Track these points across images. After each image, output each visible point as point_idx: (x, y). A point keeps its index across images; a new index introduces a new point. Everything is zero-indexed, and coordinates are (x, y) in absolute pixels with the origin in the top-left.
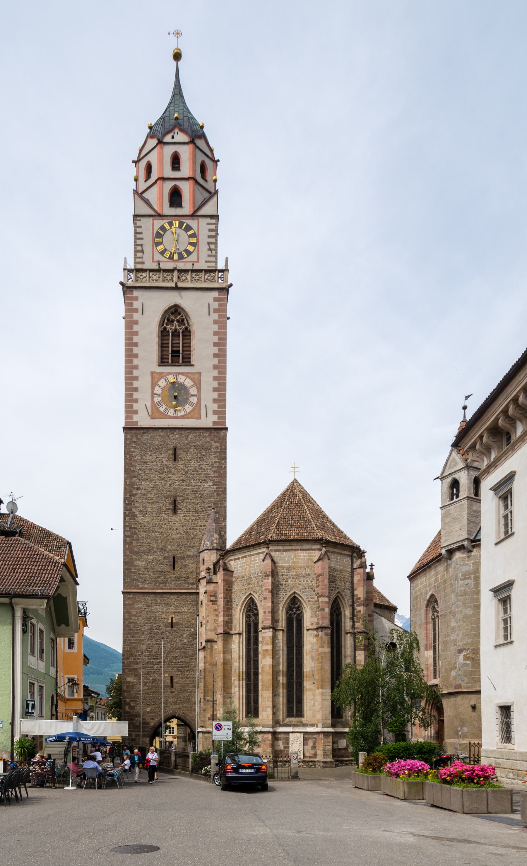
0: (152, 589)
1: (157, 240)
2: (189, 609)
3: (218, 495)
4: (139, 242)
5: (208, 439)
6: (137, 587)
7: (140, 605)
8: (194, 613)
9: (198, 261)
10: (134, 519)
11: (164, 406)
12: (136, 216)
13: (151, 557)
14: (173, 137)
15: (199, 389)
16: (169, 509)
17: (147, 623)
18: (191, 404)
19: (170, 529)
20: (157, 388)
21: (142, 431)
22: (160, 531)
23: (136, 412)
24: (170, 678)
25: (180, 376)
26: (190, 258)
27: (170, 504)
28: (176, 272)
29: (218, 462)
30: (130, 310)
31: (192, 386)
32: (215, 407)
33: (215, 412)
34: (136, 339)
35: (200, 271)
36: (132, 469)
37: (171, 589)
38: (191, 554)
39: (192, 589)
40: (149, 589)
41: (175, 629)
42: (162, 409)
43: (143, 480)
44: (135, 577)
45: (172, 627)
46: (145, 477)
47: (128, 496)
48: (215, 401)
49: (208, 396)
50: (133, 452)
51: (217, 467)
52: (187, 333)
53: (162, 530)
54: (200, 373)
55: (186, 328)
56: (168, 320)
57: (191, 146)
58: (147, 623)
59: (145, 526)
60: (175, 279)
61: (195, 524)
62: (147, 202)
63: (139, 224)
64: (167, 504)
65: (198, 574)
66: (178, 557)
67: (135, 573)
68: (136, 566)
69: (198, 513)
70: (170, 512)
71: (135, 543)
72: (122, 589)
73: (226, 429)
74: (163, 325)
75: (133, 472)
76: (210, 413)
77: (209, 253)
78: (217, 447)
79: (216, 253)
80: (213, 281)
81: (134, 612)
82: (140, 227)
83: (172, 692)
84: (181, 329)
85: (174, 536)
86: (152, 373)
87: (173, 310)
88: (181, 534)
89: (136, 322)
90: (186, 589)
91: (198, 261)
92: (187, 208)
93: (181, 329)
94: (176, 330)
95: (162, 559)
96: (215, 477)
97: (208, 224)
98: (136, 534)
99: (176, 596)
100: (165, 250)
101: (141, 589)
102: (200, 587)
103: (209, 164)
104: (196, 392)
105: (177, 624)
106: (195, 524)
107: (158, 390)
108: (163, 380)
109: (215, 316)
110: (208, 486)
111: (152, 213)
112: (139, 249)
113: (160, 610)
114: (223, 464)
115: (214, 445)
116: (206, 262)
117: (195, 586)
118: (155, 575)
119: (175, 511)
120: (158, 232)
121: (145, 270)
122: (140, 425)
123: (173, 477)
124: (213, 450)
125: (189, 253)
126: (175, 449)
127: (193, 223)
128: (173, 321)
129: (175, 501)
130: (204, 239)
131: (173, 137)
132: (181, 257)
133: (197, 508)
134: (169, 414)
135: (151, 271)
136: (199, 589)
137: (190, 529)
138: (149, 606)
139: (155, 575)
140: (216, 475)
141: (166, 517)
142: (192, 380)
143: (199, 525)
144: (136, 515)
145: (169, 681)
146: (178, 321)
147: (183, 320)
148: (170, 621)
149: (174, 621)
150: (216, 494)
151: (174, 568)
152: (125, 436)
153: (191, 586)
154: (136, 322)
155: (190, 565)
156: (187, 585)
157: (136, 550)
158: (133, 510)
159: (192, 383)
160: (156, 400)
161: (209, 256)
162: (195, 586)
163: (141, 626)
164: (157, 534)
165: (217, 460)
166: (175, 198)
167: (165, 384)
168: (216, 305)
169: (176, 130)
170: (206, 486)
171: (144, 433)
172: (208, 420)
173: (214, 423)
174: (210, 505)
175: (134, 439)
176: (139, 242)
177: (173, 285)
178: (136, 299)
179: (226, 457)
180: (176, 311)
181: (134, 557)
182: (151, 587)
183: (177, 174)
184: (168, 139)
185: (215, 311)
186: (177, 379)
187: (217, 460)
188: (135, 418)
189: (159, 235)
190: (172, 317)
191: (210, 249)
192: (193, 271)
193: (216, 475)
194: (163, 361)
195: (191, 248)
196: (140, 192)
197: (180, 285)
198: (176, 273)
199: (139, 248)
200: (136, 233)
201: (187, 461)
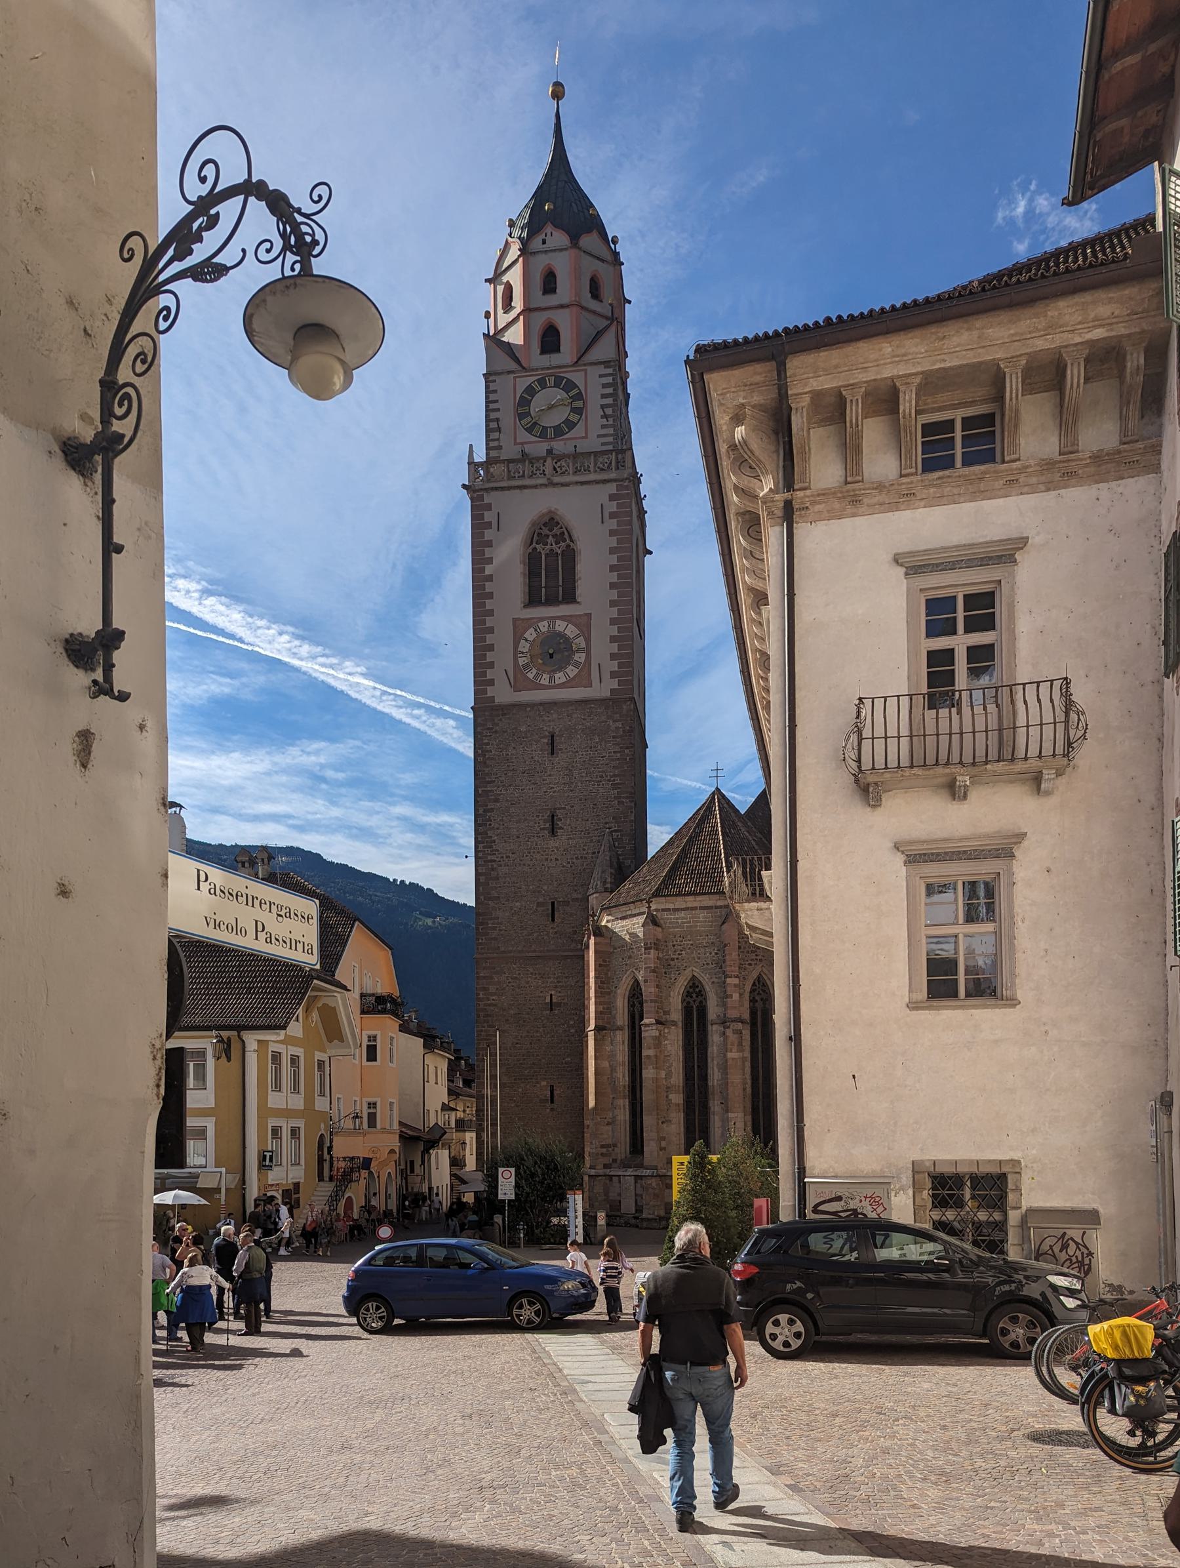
4: (493, 415)
9: (586, 437)
11: (534, 671)
14: (544, 242)
15: (588, 641)
22: (531, 863)
23: (491, 682)
25: (558, 622)
27: (545, 821)
31: (578, 636)
42: (531, 676)
50: (488, 744)
52: (570, 556)
60: (548, 470)
67: (494, 929)
71: (492, 884)
74: (531, 543)
77: (604, 422)
82: (495, 392)
83: (552, 1109)
86: (515, 620)
87: (546, 519)
91: (586, 437)
97: (600, 376)
105: (559, 1004)
107: (524, 646)
112: (493, 427)
116: (599, 436)
118: (525, 932)
119: (553, 832)
130: (595, 400)
131: (544, 242)
132: (559, 432)
139: (525, 932)
149: (554, 1000)
151: (553, 920)
157: (494, 894)
158: (490, 833)
160: (521, 661)
161: (603, 427)
164: (526, 869)
168: (613, 507)
175: (489, 725)
176: (493, 415)
183: (552, 300)
185: (613, 515)
186: (554, 626)
190: (545, 531)
191: (605, 416)
194: (533, 600)
195: (574, 418)
197: (556, 479)
199: (493, 425)
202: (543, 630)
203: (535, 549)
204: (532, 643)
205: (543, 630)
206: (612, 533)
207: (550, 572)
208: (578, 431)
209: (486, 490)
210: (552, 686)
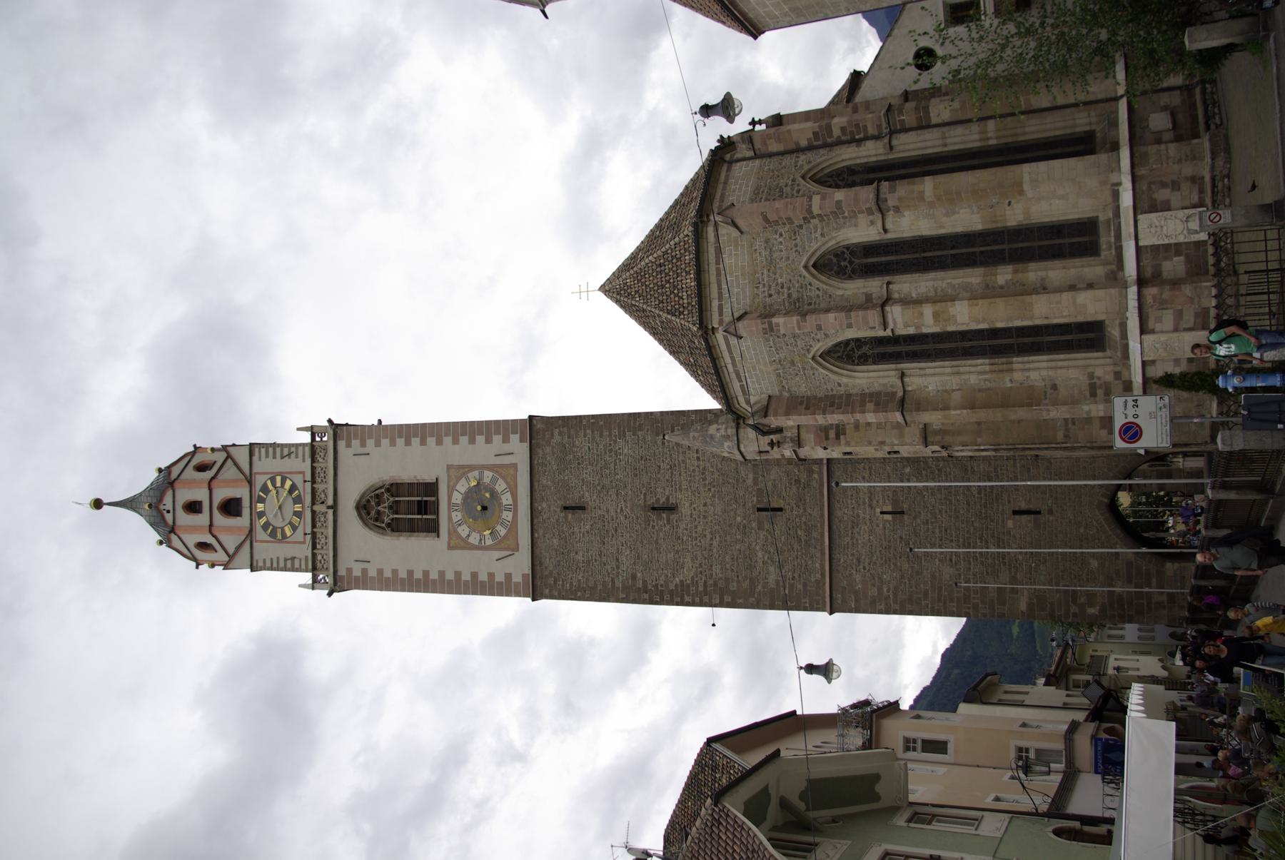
0: (823, 553)
1: (279, 536)
3: (640, 428)
4: (282, 565)
5: (548, 449)
6: (819, 583)
7: (858, 577)
9: (303, 473)
10: (688, 586)
12: (253, 569)
13: (760, 554)
15: (472, 468)
16: (668, 520)
17: (895, 565)
18: (494, 480)
19: (705, 517)
20: (471, 540)
21: (538, 568)
22: (709, 536)
24: (1017, 517)
25: (454, 501)
26: (300, 484)
27: (660, 518)
28: (315, 508)
30: (363, 582)
32: (497, 439)
33: (506, 440)
34: (403, 574)
35: (313, 469)
36: (600, 587)
37: (822, 516)
38: (751, 476)
39: (821, 474)
40: (823, 560)
41: (905, 506)
43: (618, 567)
44: (800, 587)
45: (903, 513)
46: (614, 564)
47: (646, 596)
48: (489, 440)
49: (483, 453)
52: (395, 488)
53: (707, 533)
54: (449, 467)
55: (388, 490)
56: (377, 520)
57: (177, 484)
58: (895, 565)
59: (701, 566)
62: (238, 548)
63: (260, 564)
64: (661, 523)
65: (790, 461)
66: (758, 502)
67: (791, 586)
68: (778, 585)
70: (674, 517)
72: (826, 614)
73: (531, 417)
75: (604, 584)
76: (506, 448)
77: (293, 456)
78: (560, 434)
79: (293, 445)
80: (325, 449)
81: (873, 592)
83: (1050, 512)
84: (388, 500)
85: (719, 510)
86: (450, 548)
87: (363, 512)
88: (713, 496)
89: (380, 572)
90: (822, 485)
91: (303, 473)
92: (242, 492)
93: (388, 500)
94: (390, 507)
95: (762, 534)
96: (610, 435)
98: (715, 584)
99: (837, 505)
100: (290, 523)
101: (823, 575)
102: (816, 457)
103: (198, 459)
104: (476, 473)
105: (895, 502)
107: (474, 539)
108: (460, 529)
109: (370, 443)
110: (627, 448)
111: (248, 542)
112: (289, 565)
113: (866, 536)
115: (557, 438)
117: (815, 468)
119: (671, 509)
120: (270, 535)
121: (314, 555)
122: (528, 571)
123: (612, 513)
124: (566, 439)
125: (293, 488)
126: (566, 508)
127: (259, 481)
128: (378, 512)
129: (653, 509)
133: (664, 466)
134: (510, 519)
135: (314, 547)
136: (821, 460)
137: (704, 479)
138: (859, 561)
139: (796, 547)
140: (606, 433)
141: (682, 526)
142: (458, 479)
143: (696, 463)
144: (682, 582)
145: (1024, 518)
146: (378, 504)
147: (377, 496)
148: (889, 517)
149: (889, 509)
151: (780, 510)
152: (547, 597)
153: (816, 476)
154: (380, 572)
156: (814, 483)
157: (746, 584)
158: (672, 587)
159: (463, 481)
160: (489, 542)
162: (815, 468)
163: (902, 577)
164: (715, 543)
166: (231, 507)
167: (464, 527)
169: (162, 507)
171: (541, 564)
172: (519, 451)
173: (522, 441)
174: (659, 443)
175: (551, 581)
176: (282, 565)
177: (331, 512)
178: (349, 570)
180: (365, 507)
181: (760, 587)
182: (818, 555)
184: (169, 517)
185: (363, 445)
186: (457, 505)
188: (517, 578)
189: (273, 534)
190: (373, 513)
191: (289, 455)
192: (313, 481)
193: (606, 433)
194: (432, 528)
195: (288, 484)
196: (227, 559)
197: (330, 502)
198: (315, 508)
200: (272, 569)
202: (460, 517)
203: (389, 525)
204: (472, 530)
205: (460, 517)
206: (378, 444)
207: (406, 509)
208: (298, 480)
209: (335, 572)
210: (514, 508)
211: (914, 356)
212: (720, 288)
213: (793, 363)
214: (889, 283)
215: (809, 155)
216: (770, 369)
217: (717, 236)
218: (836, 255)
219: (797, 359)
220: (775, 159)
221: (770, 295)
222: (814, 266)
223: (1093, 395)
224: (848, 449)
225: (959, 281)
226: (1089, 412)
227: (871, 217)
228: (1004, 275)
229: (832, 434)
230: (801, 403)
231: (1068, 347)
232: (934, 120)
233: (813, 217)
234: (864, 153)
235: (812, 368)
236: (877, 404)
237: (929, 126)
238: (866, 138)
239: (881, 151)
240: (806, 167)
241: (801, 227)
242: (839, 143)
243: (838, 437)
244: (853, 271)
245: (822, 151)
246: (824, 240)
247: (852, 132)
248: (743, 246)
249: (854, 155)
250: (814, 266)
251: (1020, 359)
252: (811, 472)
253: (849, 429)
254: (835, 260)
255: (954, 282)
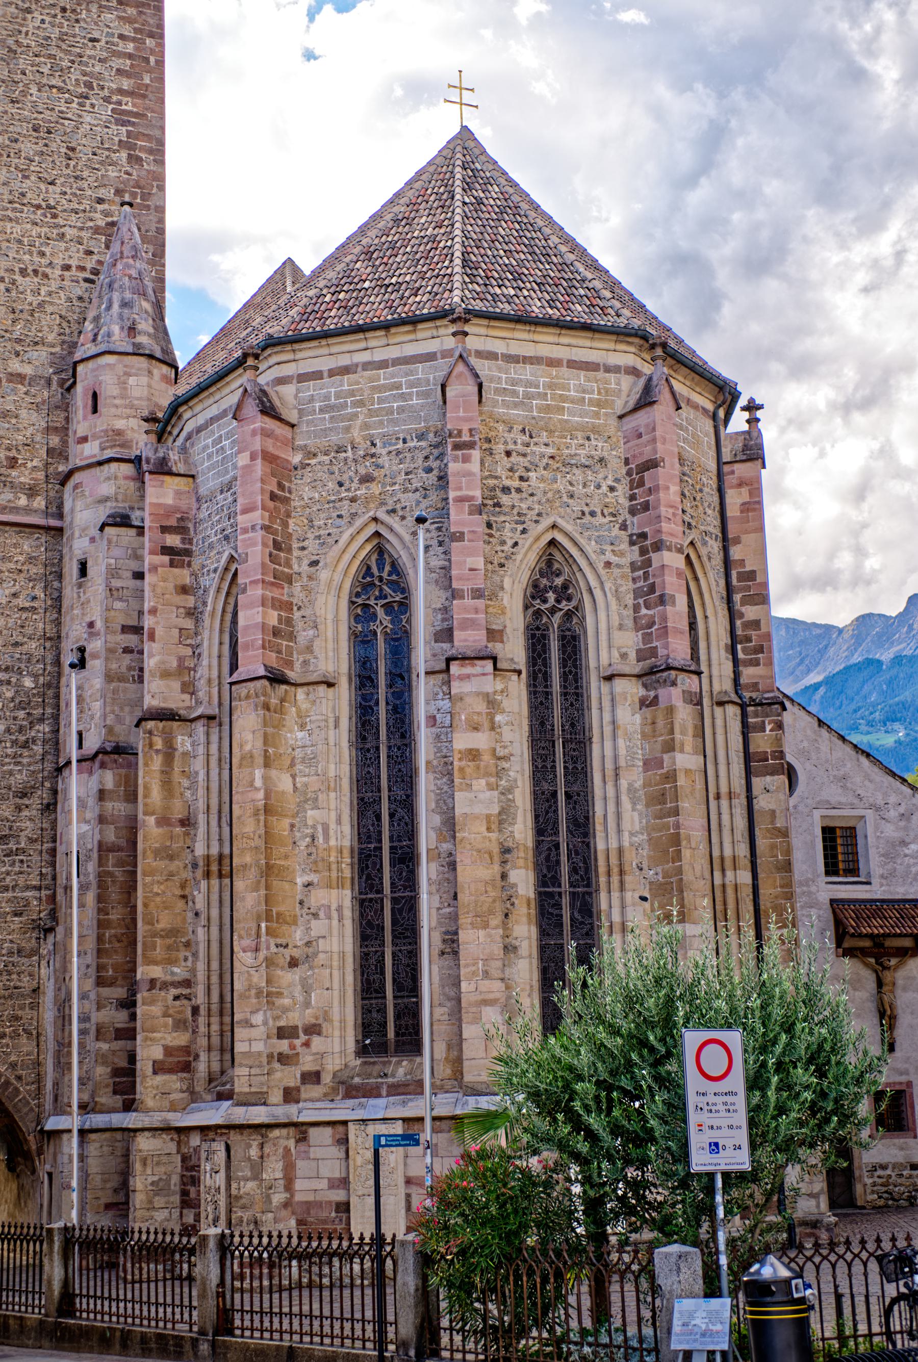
2: (15, 595)
3: (134, 159)
8: (33, 609)
29: (134, 40)
38: (28, 370)
51: (130, 56)
61: (42, 254)
69: (55, 216)
96: (121, 91)
106: (42, 254)
114: (152, 52)
117: (39, 503)
133: (53, 194)
137: (23, 272)
140: (126, 84)
143: (58, 261)
150: (124, 155)
153: (23, 501)
155: (23, 413)
165: (127, 30)
170: (88, 118)
174: (102, 193)
179: (161, 26)
187: (127, 30)
193: (126, 84)
201: (12, 9)
211: (364, 711)
212: (526, 360)
213: (367, 479)
214: (519, 672)
215: (718, 560)
216: (356, 434)
217: (616, 369)
218: (565, 587)
219: (375, 488)
220: (716, 499)
221: (508, 454)
222: (553, 543)
223: (282, 1033)
224: (96, 571)
225: (519, 802)
226: (248, 1024)
227: (633, 655)
228: (524, 881)
229: (173, 540)
230: (281, 486)
231: (369, 988)
232: (757, 782)
233: (643, 551)
234: (714, 656)
235: (354, 515)
236: (276, 632)
237: (748, 773)
238: (736, 662)
239: (716, 687)
240: (703, 551)
241: (624, 527)
242: (732, 615)
243: (166, 550)
244: (538, 614)
245: (722, 582)
246: (600, 566)
247: (748, 639)
248: (597, 415)
249: (713, 639)
250: (553, 543)
251: (347, 903)
252: (32, 492)
253: (184, 576)
254: (559, 581)
255: (518, 793)
